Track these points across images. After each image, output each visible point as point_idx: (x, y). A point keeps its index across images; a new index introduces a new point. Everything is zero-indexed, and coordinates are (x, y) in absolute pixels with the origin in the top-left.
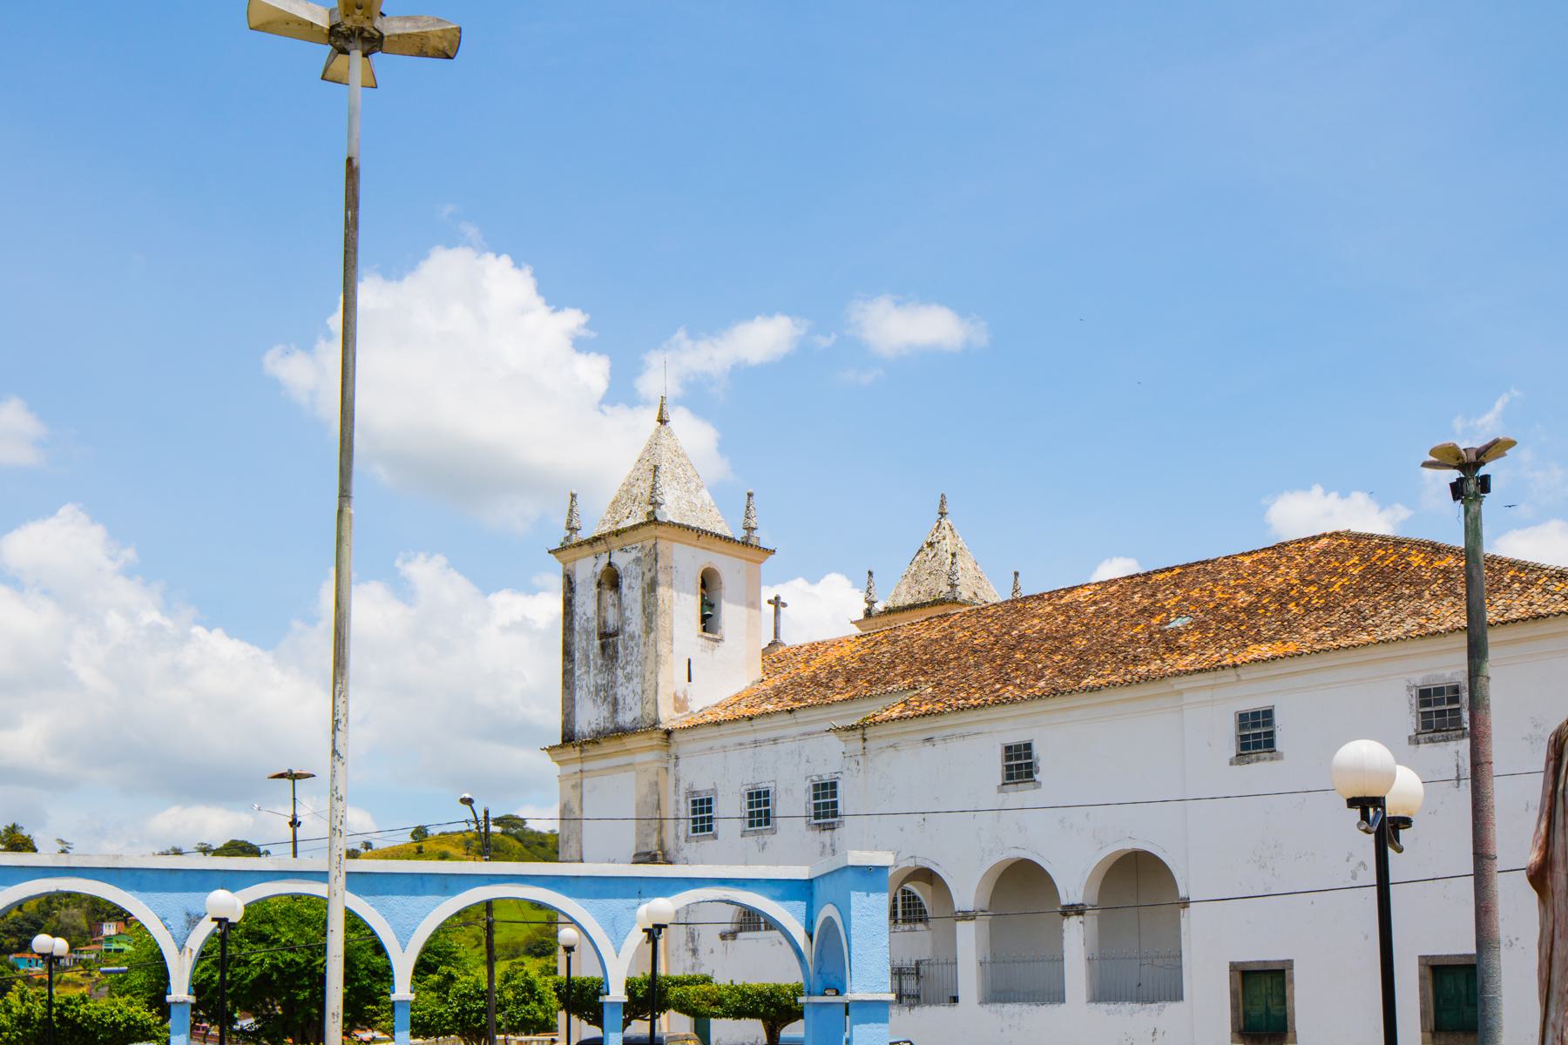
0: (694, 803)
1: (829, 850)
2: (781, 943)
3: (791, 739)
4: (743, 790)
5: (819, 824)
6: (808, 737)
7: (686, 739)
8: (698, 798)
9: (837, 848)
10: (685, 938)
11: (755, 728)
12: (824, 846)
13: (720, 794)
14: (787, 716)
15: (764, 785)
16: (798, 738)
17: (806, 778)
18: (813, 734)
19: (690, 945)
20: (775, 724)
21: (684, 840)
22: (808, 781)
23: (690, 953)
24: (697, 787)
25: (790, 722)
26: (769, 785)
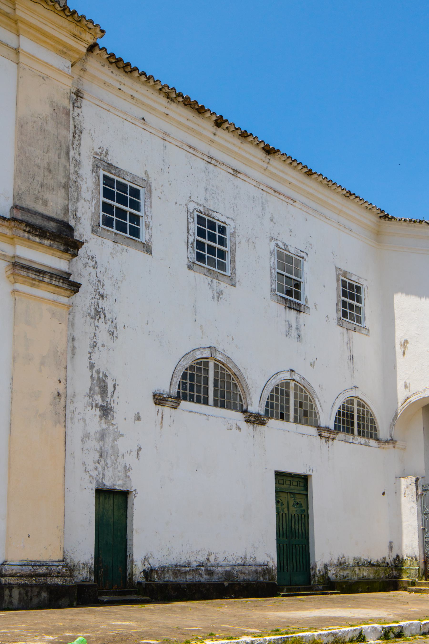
0: (107, 180)
1: (294, 333)
2: (239, 429)
3: (255, 183)
4: (192, 206)
5: (286, 299)
6: (272, 192)
7: (107, 79)
8: (116, 178)
9: (302, 333)
10: (89, 384)
11: (216, 138)
12: (290, 327)
13: (154, 192)
14: (261, 154)
15: (223, 219)
16: (261, 187)
17: (271, 239)
18: (280, 194)
19: (98, 399)
20: (244, 154)
21: (89, 229)
22: (273, 243)
23: (98, 412)
24: (113, 159)
25: (261, 163)
26: (228, 221)
